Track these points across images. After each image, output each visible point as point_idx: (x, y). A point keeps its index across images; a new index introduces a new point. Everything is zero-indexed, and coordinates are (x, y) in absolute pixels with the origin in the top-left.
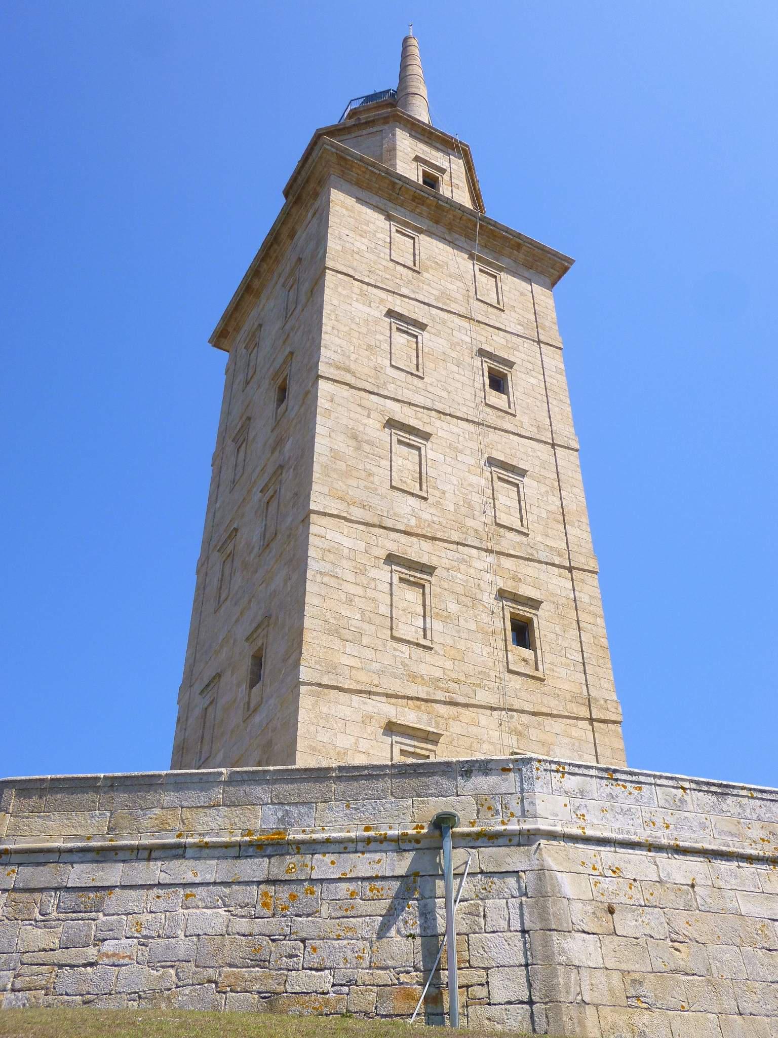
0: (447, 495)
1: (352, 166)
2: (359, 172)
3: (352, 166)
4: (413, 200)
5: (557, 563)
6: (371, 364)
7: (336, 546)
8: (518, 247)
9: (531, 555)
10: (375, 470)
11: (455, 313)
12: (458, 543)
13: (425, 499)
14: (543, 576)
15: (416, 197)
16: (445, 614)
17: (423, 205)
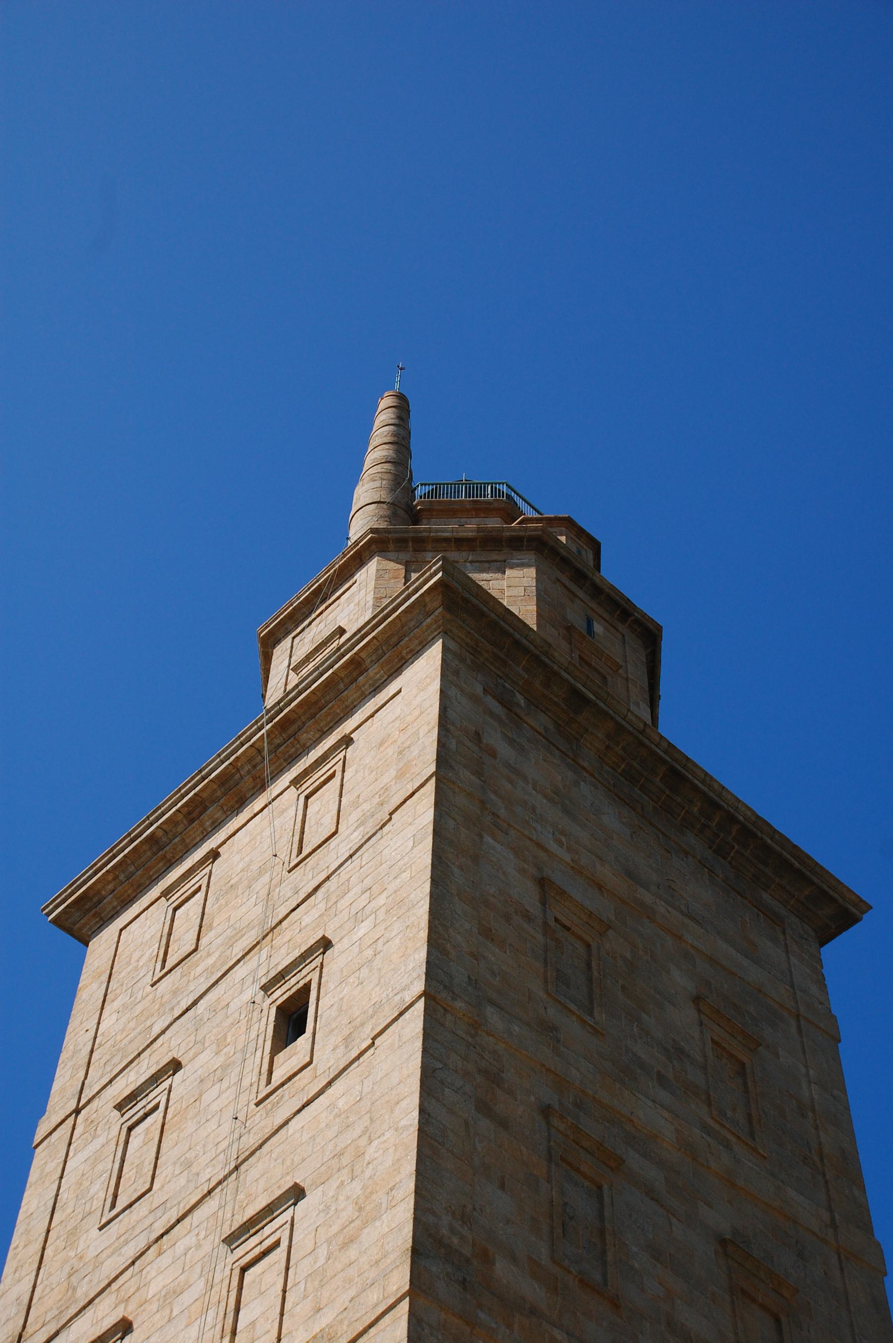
1: (99, 892)
2: (110, 887)
3: (99, 892)
4: (192, 821)
15: (189, 813)
17: (206, 808)
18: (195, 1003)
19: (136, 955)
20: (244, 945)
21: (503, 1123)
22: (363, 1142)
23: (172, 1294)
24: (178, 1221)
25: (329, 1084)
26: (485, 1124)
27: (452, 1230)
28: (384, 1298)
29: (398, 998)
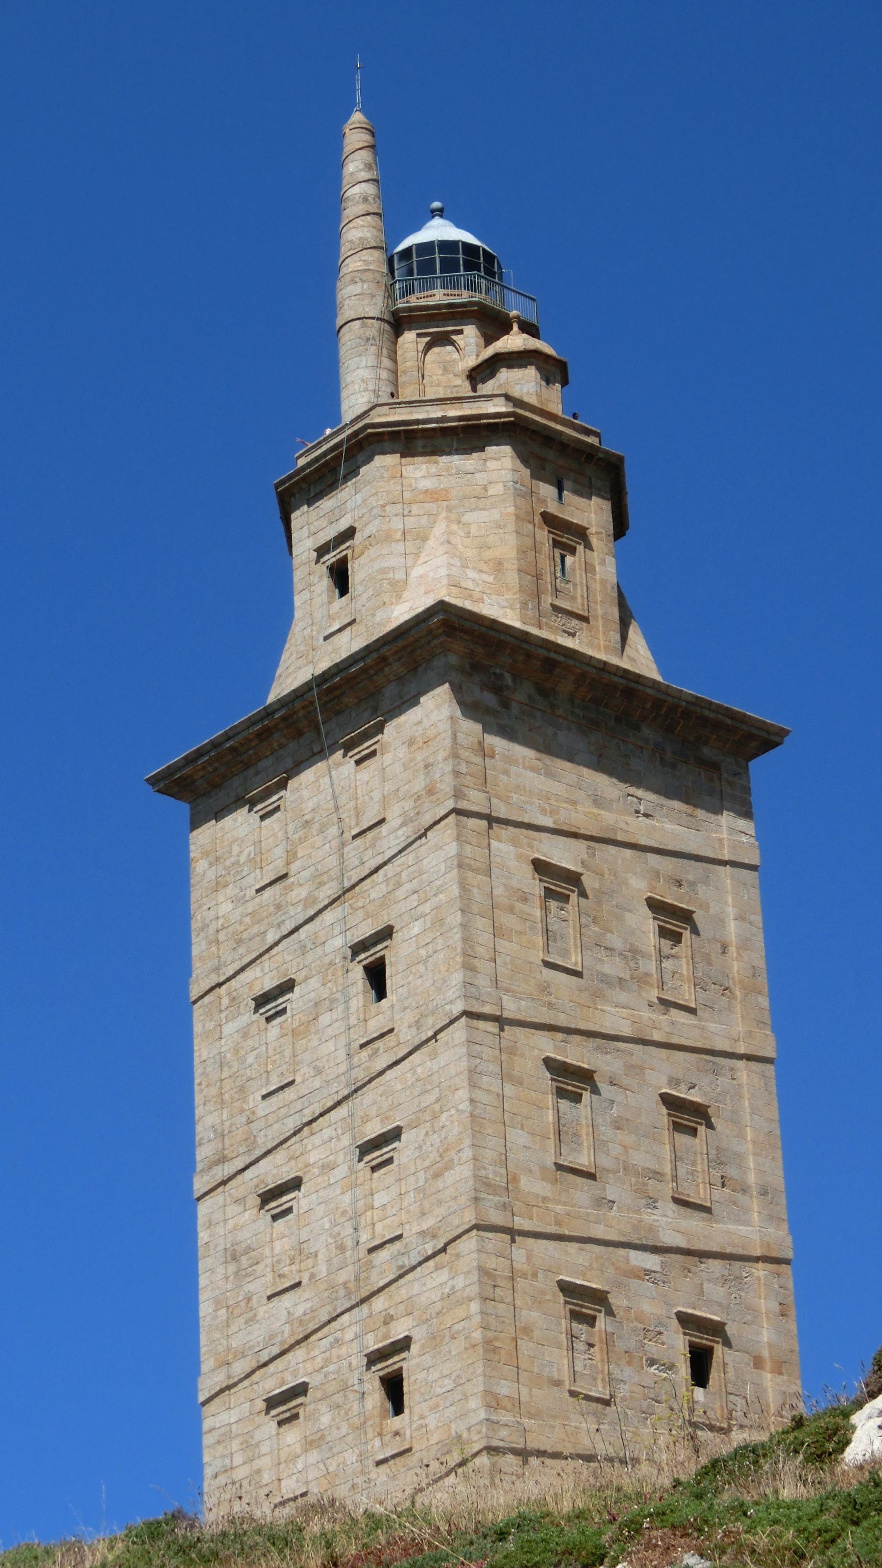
0: (320, 1256)
5: (430, 1252)
6: (244, 1120)
7: (223, 1430)
8: (383, 660)
9: (402, 1267)
10: (251, 1287)
11: (326, 907)
12: (329, 1322)
13: (298, 1284)
14: (416, 1289)
16: (319, 1434)
18: (296, 929)
19: (236, 849)
20: (330, 892)
21: (520, 1083)
22: (437, 1107)
23: (328, 1168)
24: (321, 1115)
25: (410, 1053)
26: (509, 1090)
27: (495, 1172)
28: (463, 1224)
29: (447, 1007)
